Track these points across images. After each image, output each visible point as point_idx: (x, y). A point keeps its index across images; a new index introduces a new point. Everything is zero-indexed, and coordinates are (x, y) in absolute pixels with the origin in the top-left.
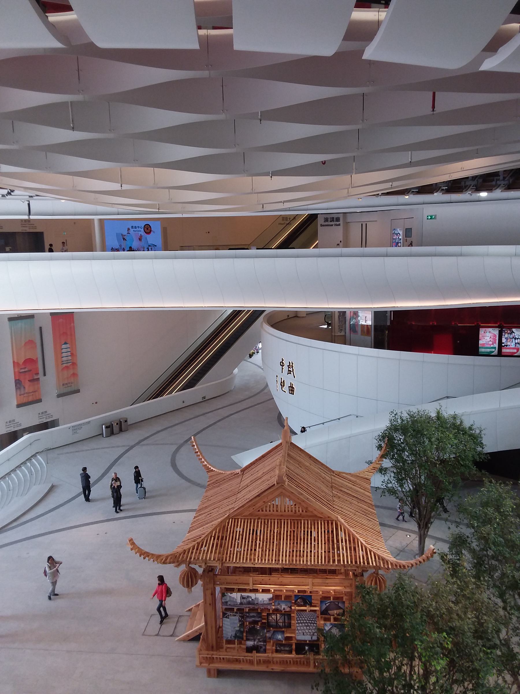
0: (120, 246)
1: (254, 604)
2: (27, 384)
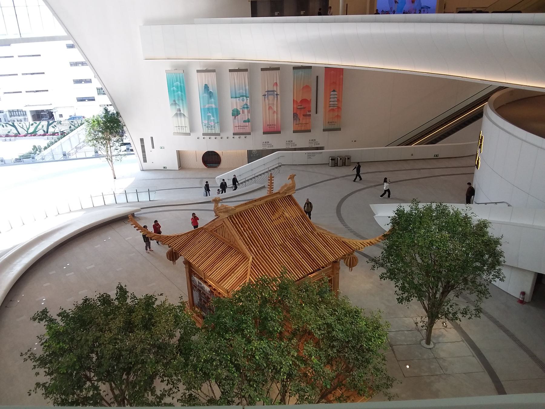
0: (391, 8)
2: (301, 117)
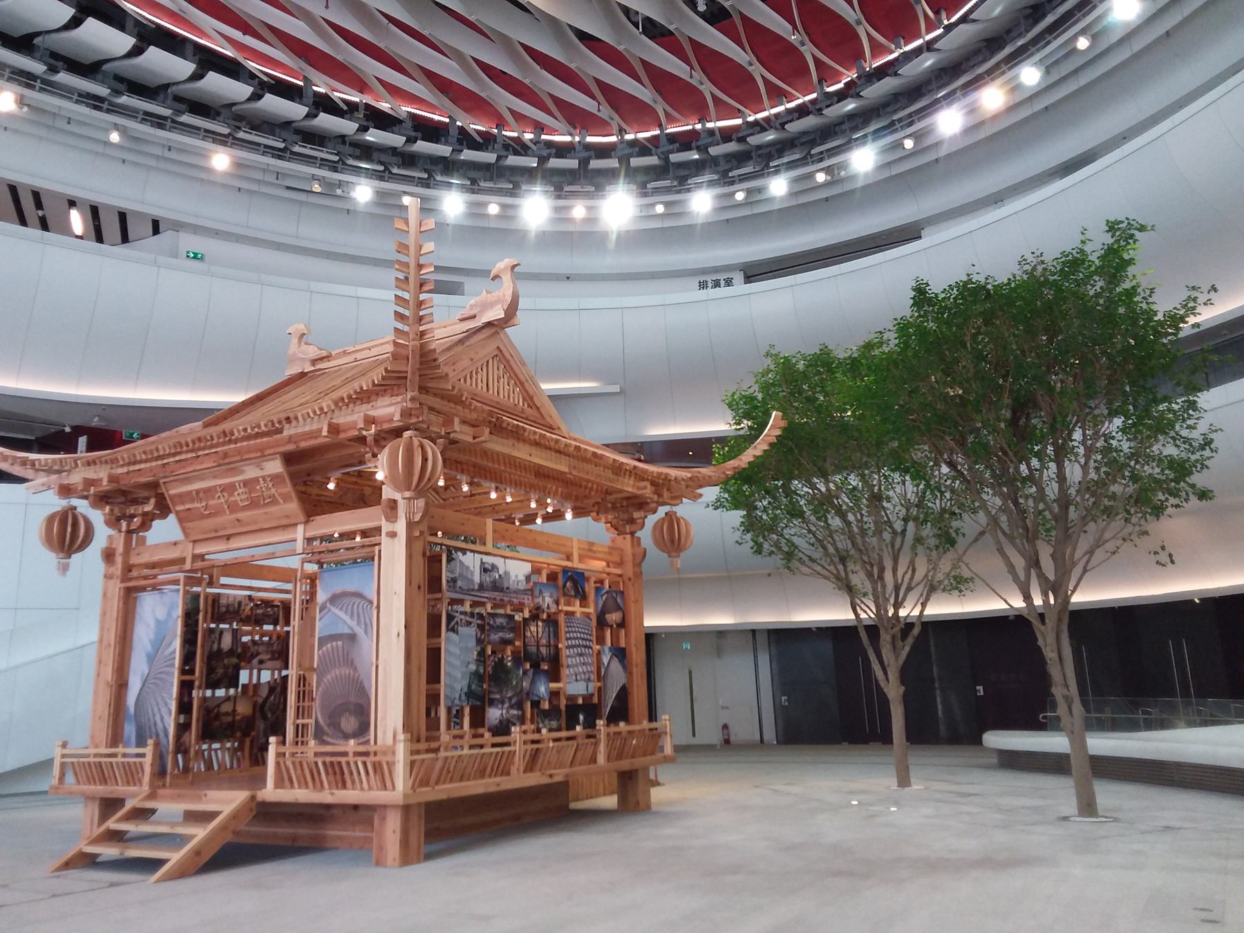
1: (501, 590)
